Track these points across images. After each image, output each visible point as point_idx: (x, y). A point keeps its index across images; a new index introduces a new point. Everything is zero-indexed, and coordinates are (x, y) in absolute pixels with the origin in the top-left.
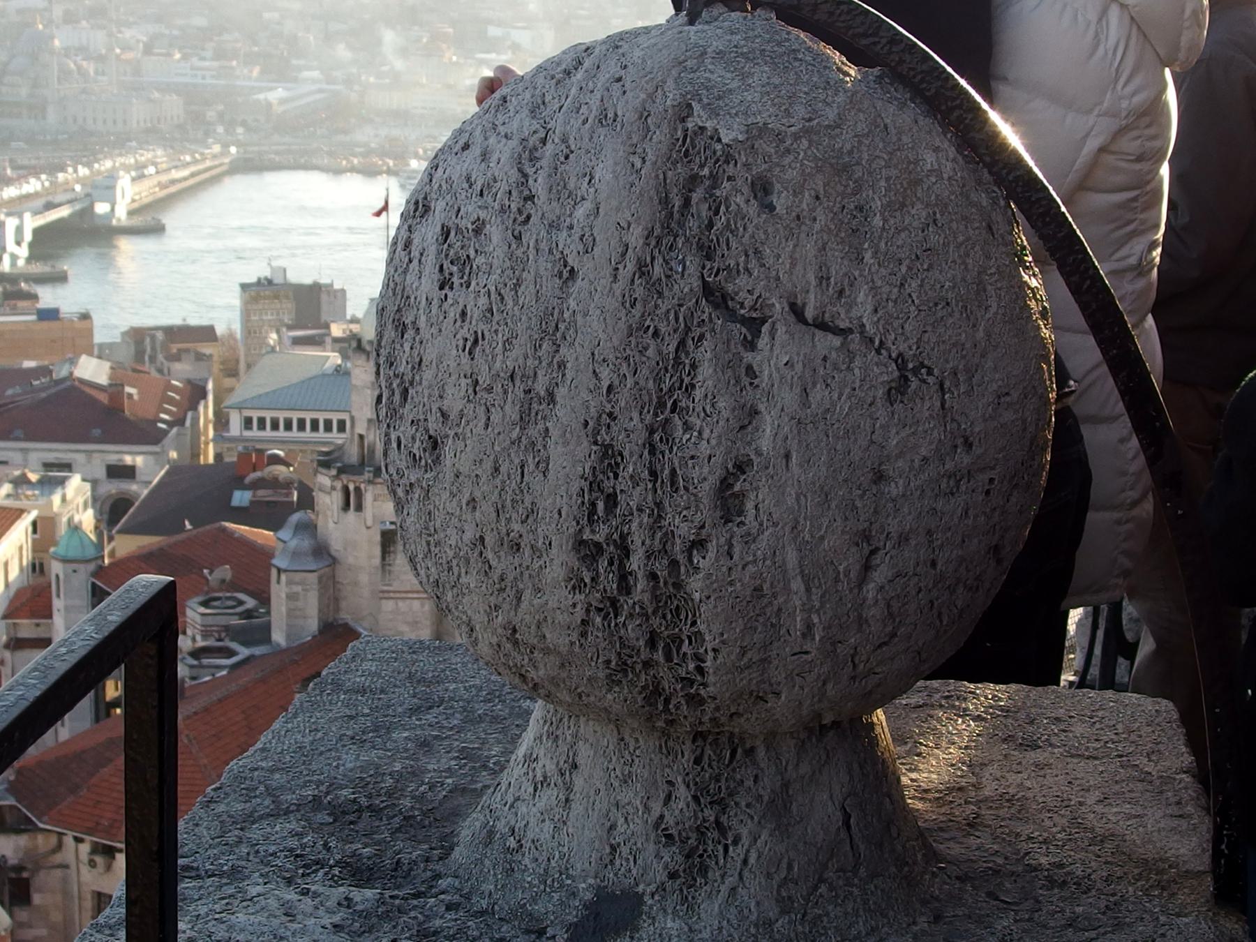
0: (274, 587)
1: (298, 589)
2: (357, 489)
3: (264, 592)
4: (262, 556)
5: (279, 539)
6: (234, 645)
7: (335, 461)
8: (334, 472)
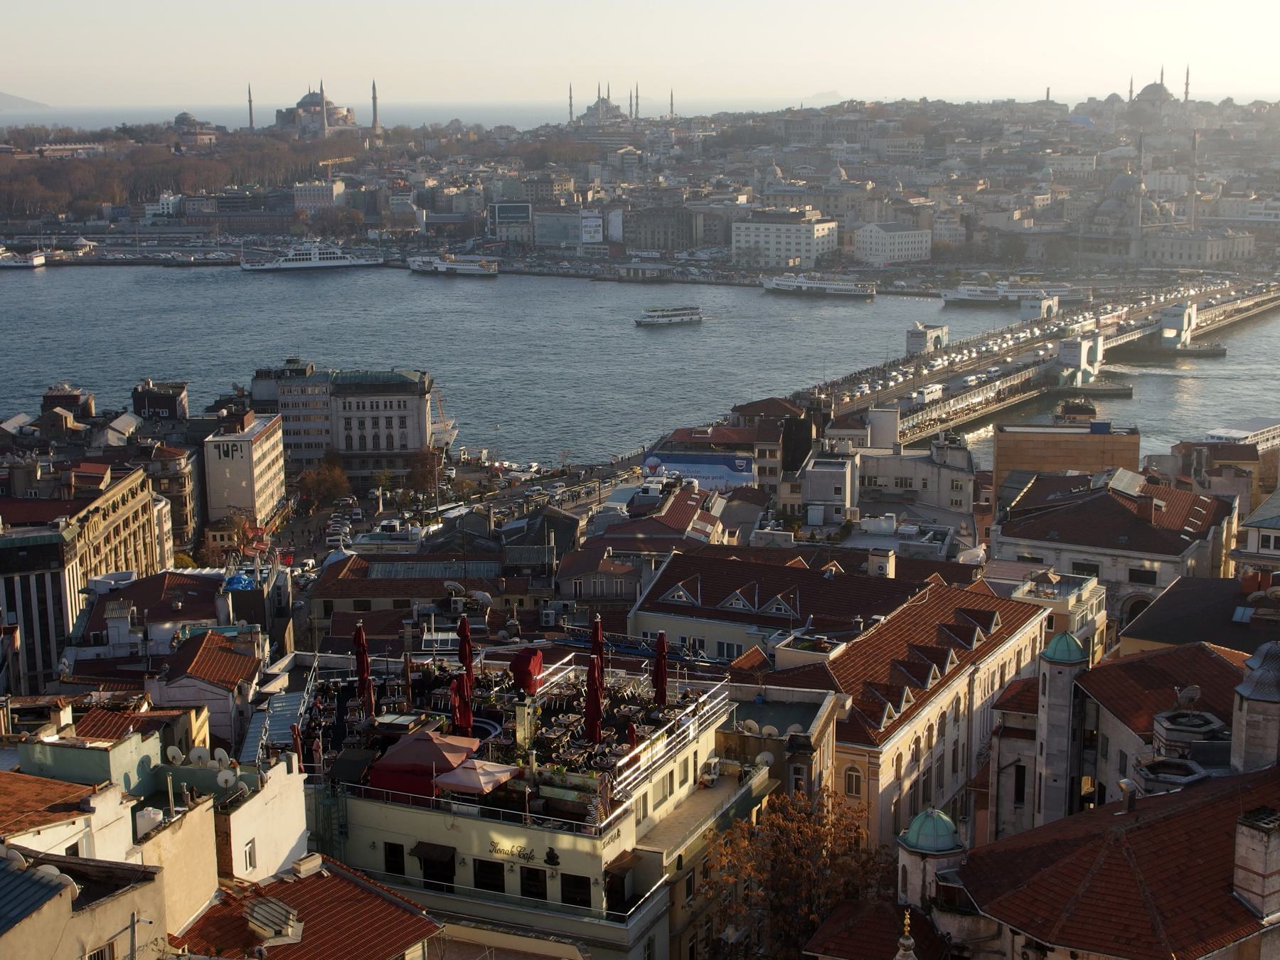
0: (1236, 713)
6: (1192, 764)
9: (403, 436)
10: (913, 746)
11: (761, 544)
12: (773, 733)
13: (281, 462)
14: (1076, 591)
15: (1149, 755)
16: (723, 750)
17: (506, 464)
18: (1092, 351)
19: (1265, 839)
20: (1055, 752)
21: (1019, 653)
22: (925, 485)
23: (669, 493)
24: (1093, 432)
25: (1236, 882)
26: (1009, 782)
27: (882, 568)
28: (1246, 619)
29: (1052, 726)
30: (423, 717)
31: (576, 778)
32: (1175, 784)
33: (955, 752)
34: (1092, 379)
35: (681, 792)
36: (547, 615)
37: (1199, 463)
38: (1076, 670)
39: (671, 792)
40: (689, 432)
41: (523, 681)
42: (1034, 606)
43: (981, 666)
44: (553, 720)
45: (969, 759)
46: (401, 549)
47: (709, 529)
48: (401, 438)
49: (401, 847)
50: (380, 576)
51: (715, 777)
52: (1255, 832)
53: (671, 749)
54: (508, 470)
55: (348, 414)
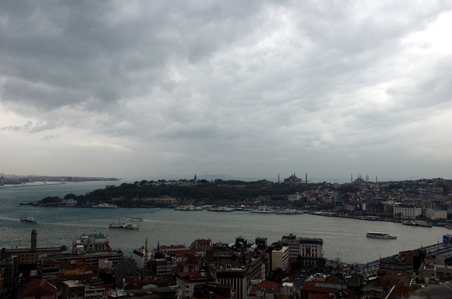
9: (316, 254)
13: (288, 258)
50: (318, 286)
55: (303, 248)
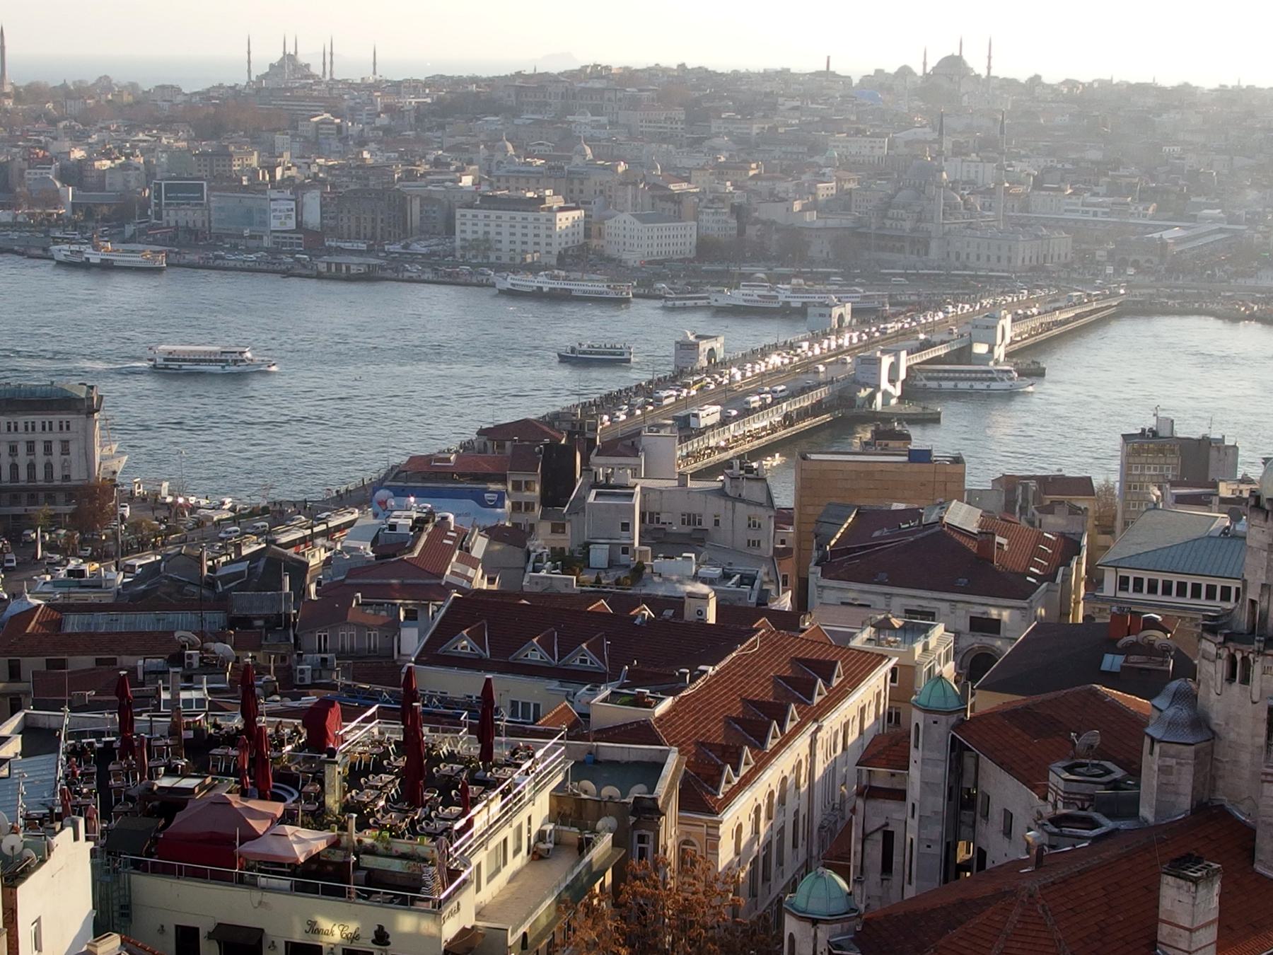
0: (1146, 757)
1: (1174, 761)
2: (1245, 659)
3: (1135, 763)
4: (1137, 723)
5: (1153, 706)
6: (1098, 816)
7: (1222, 626)
8: (1221, 639)
10: (753, 816)
11: (538, 589)
12: (614, 795)
14: (922, 639)
15: (1048, 810)
16: (558, 815)
17: (192, 500)
18: (894, 368)
19: (1193, 889)
20: (929, 814)
21: (863, 710)
22: (717, 523)
23: (422, 530)
24: (911, 461)
25: (1160, 938)
26: (875, 852)
27: (701, 613)
28: (1116, 669)
29: (925, 784)
30: (208, 780)
31: (403, 845)
32: (1084, 838)
33: (795, 824)
34: (893, 401)
35: (516, 862)
36: (302, 671)
37: (1025, 499)
38: (953, 719)
39: (505, 863)
40: (428, 459)
41: (318, 741)
42: (878, 655)
43: (825, 723)
44: (362, 780)
45: (810, 832)
46: (92, 597)
47: (471, 572)
48: (63, 468)
49: (196, 930)
51: (551, 846)
52: (1182, 882)
53: (507, 812)
54: (194, 509)
